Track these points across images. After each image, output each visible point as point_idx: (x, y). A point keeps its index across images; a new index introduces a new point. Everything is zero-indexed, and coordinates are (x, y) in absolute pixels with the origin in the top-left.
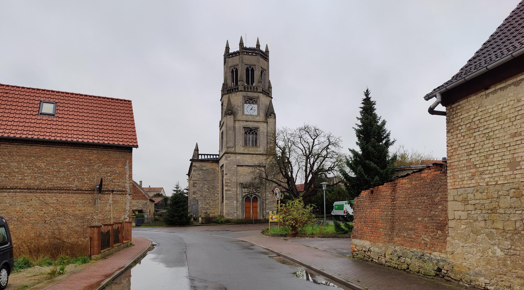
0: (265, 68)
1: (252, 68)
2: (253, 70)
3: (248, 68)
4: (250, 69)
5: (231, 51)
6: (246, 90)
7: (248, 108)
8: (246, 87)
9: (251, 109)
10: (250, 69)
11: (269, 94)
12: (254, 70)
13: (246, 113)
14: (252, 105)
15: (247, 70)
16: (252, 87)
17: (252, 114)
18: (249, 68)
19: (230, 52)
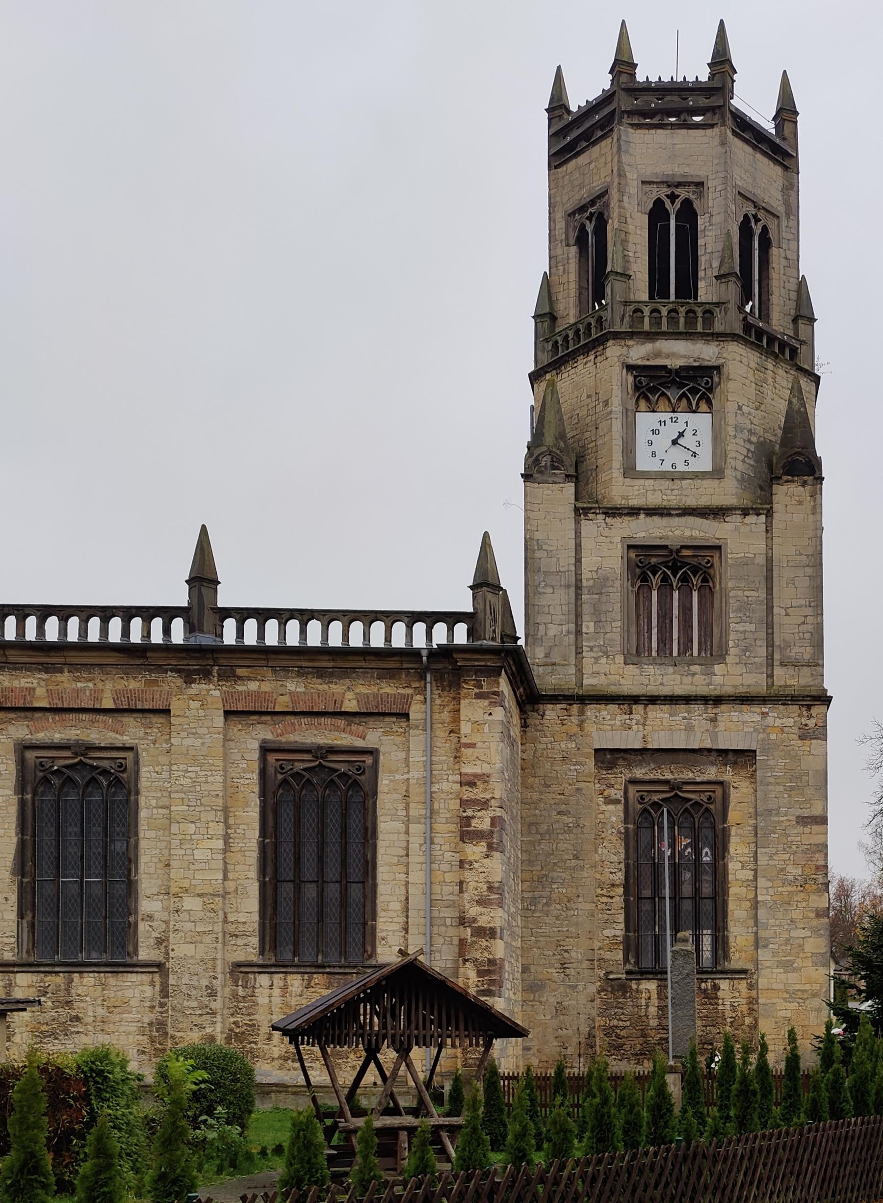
0: (773, 198)
1: (687, 203)
2: (688, 214)
3: (659, 203)
4: (672, 209)
5: (576, 101)
6: (664, 328)
7: (654, 438)
8: (647, 311)
9: (675, 442)
10: (672, 209)
11: (794, 352)
12: (695, 215)
13: (644, 463)
14: (683, 417)
15: (657, 214)
16: (664, 312)
17: (681, 467)
18: (668, 204)
19: (574, 108)
